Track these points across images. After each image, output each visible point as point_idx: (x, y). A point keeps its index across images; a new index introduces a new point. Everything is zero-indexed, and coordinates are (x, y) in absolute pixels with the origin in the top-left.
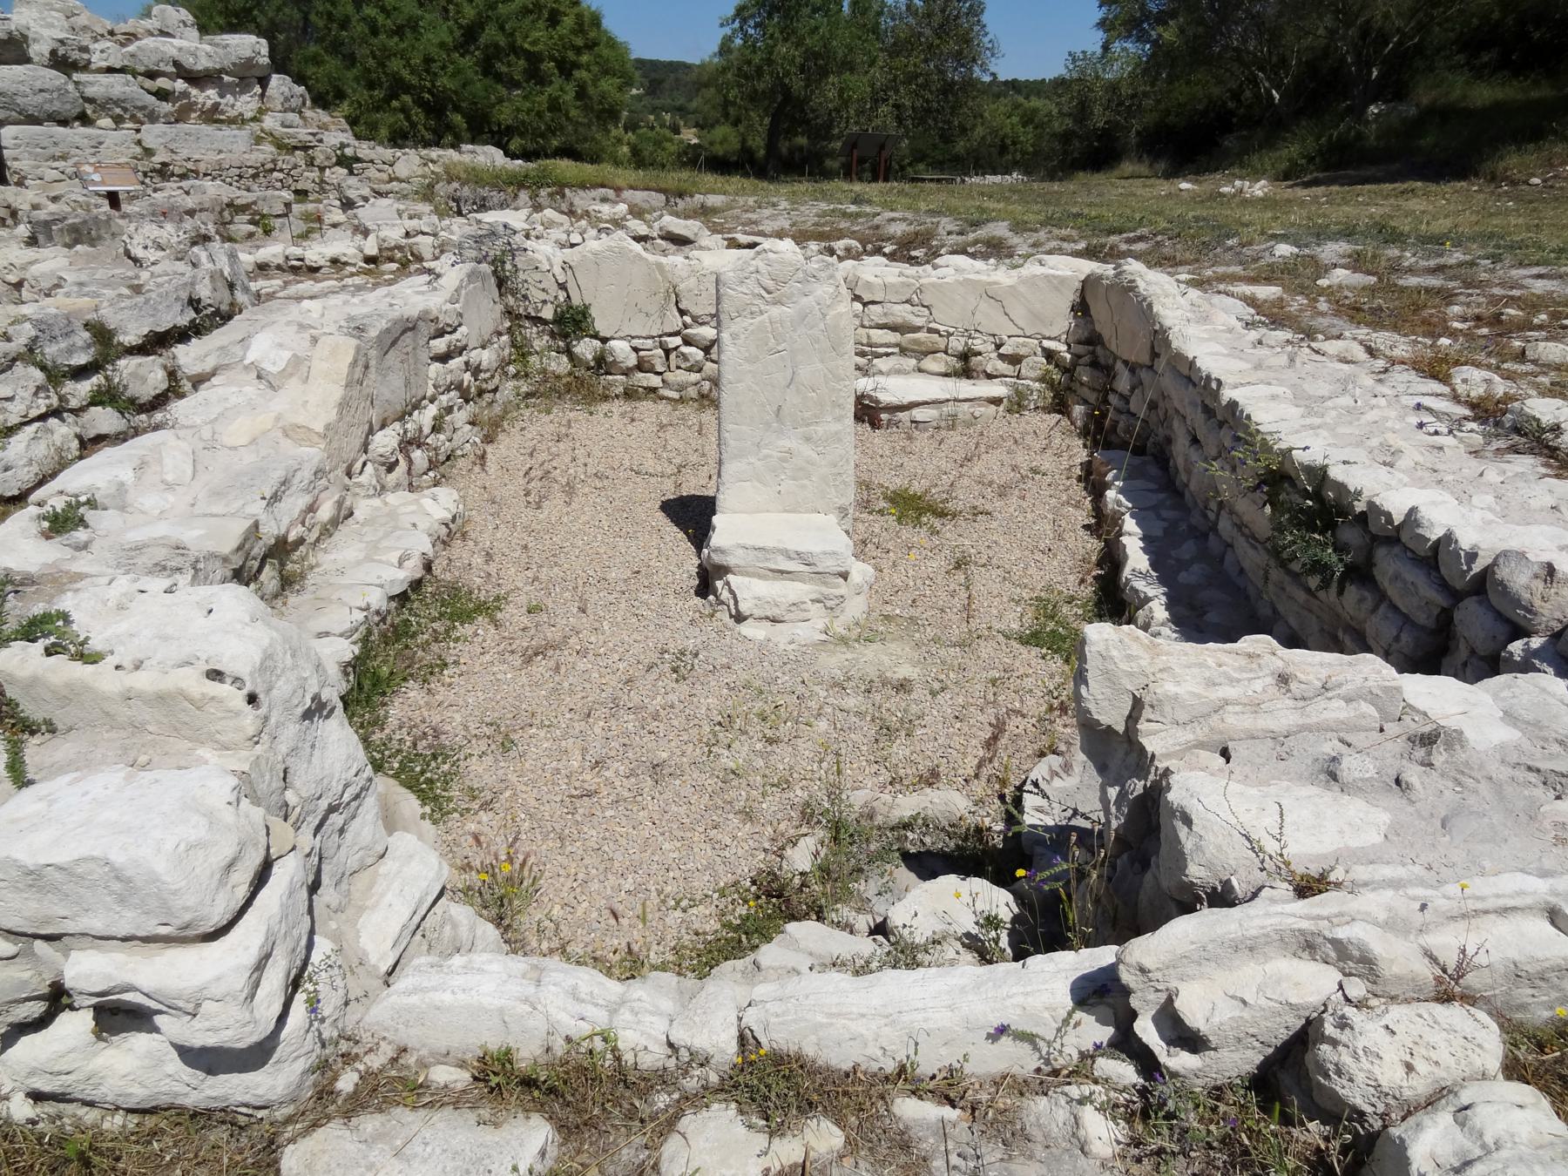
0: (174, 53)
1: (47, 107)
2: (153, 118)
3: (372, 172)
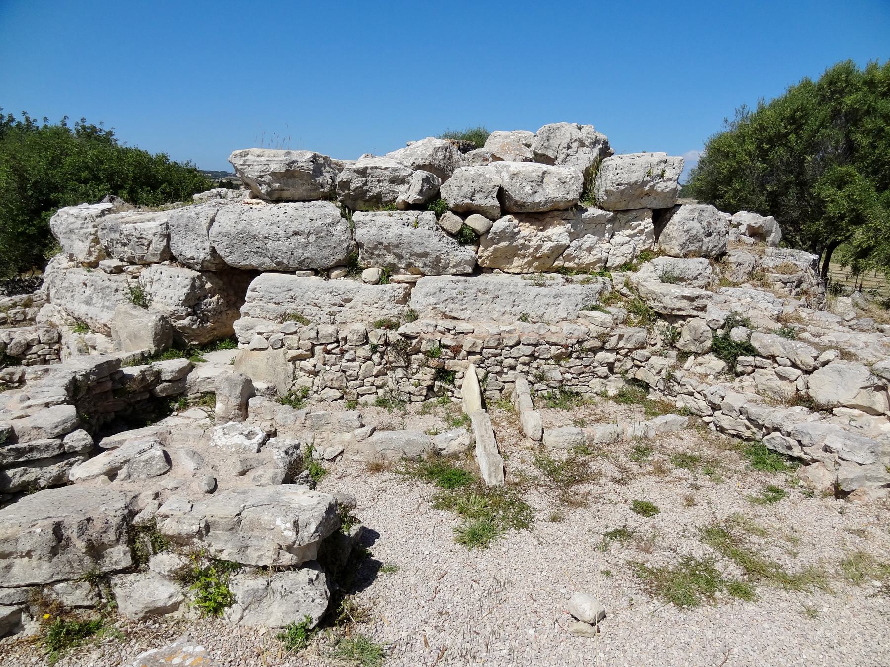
0: (504, 180)
1: (298, 252)
2: (438, 268)
3: (767, 377)
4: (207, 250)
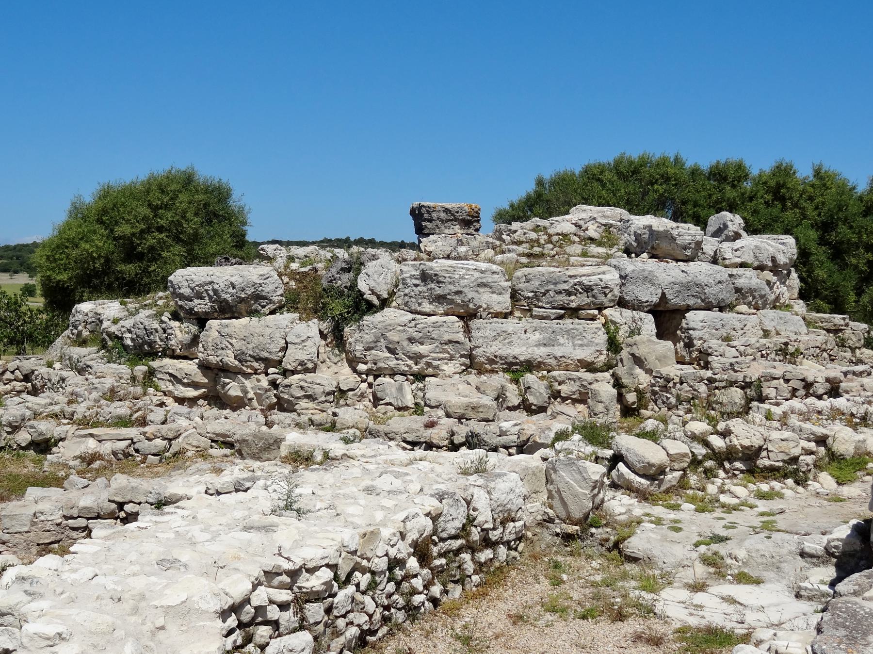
4: (659, 296)
